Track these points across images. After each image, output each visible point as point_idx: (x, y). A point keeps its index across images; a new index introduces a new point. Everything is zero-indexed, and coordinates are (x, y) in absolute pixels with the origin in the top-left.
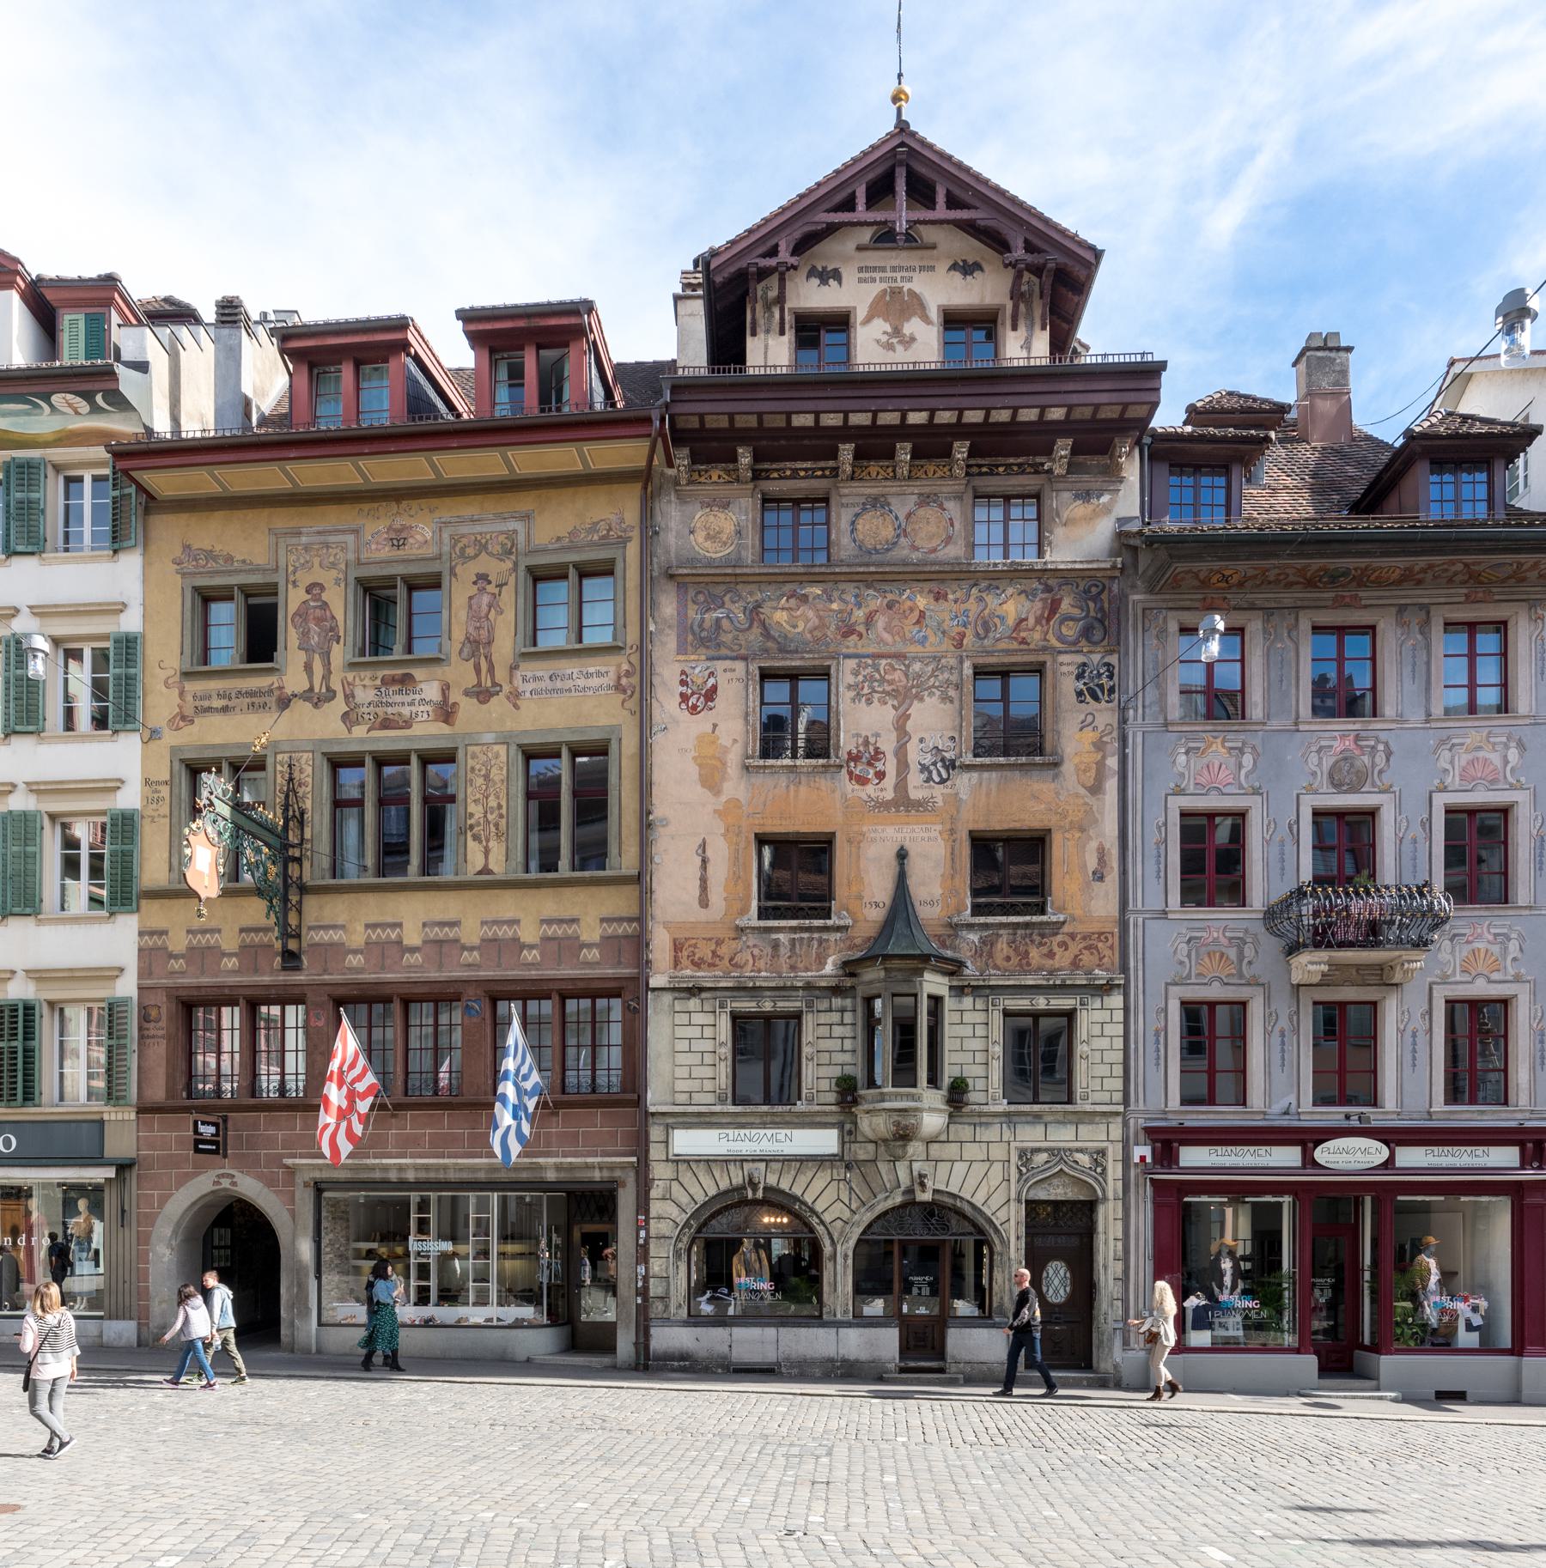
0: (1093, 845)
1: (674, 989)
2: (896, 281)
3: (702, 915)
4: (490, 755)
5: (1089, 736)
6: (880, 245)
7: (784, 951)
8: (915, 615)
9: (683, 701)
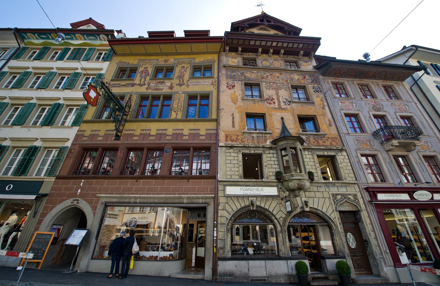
0: (327, 119)
1: (226, 146)
5: (319, 99)
8: (276, 77)
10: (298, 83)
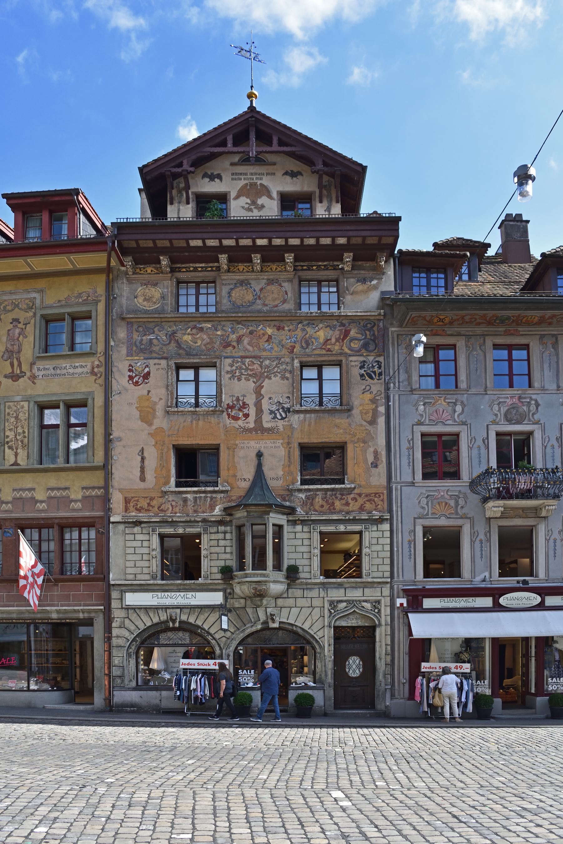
0: (372, 449)
1: (125, 523)
2: (253, 179)
3: (142, 485)
4: (18, 407)
5: (368, 396)
6: (243, 163)
7: (190, 503)
9: (130, 380)
10: (324, 352)
